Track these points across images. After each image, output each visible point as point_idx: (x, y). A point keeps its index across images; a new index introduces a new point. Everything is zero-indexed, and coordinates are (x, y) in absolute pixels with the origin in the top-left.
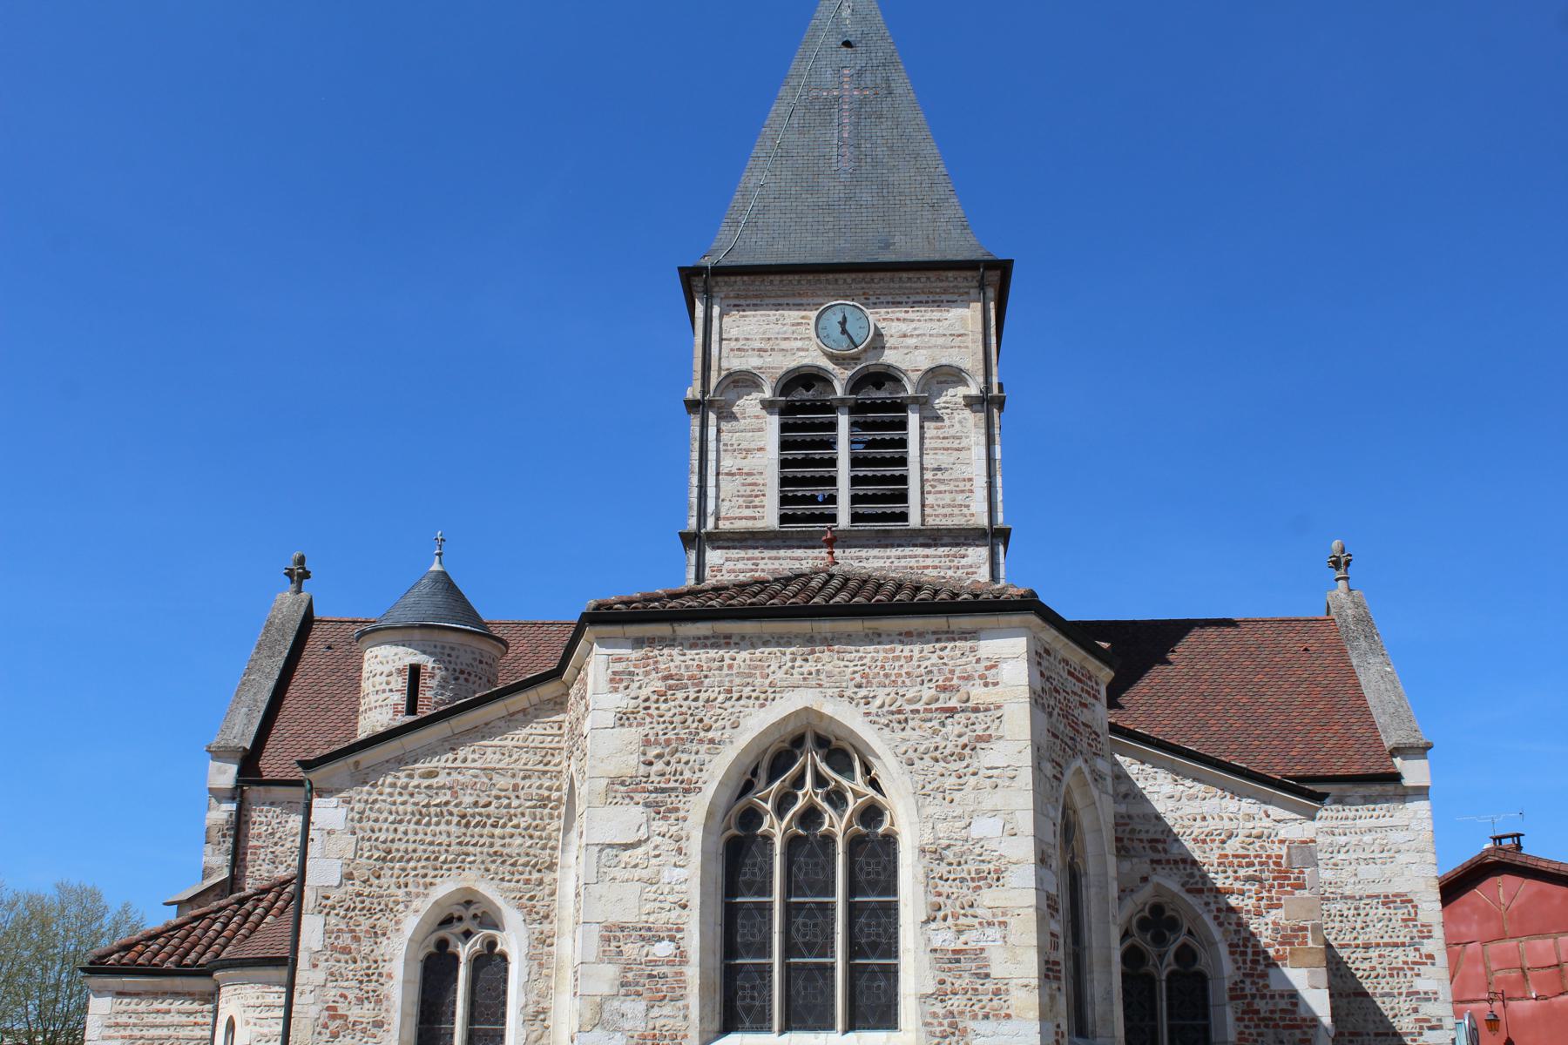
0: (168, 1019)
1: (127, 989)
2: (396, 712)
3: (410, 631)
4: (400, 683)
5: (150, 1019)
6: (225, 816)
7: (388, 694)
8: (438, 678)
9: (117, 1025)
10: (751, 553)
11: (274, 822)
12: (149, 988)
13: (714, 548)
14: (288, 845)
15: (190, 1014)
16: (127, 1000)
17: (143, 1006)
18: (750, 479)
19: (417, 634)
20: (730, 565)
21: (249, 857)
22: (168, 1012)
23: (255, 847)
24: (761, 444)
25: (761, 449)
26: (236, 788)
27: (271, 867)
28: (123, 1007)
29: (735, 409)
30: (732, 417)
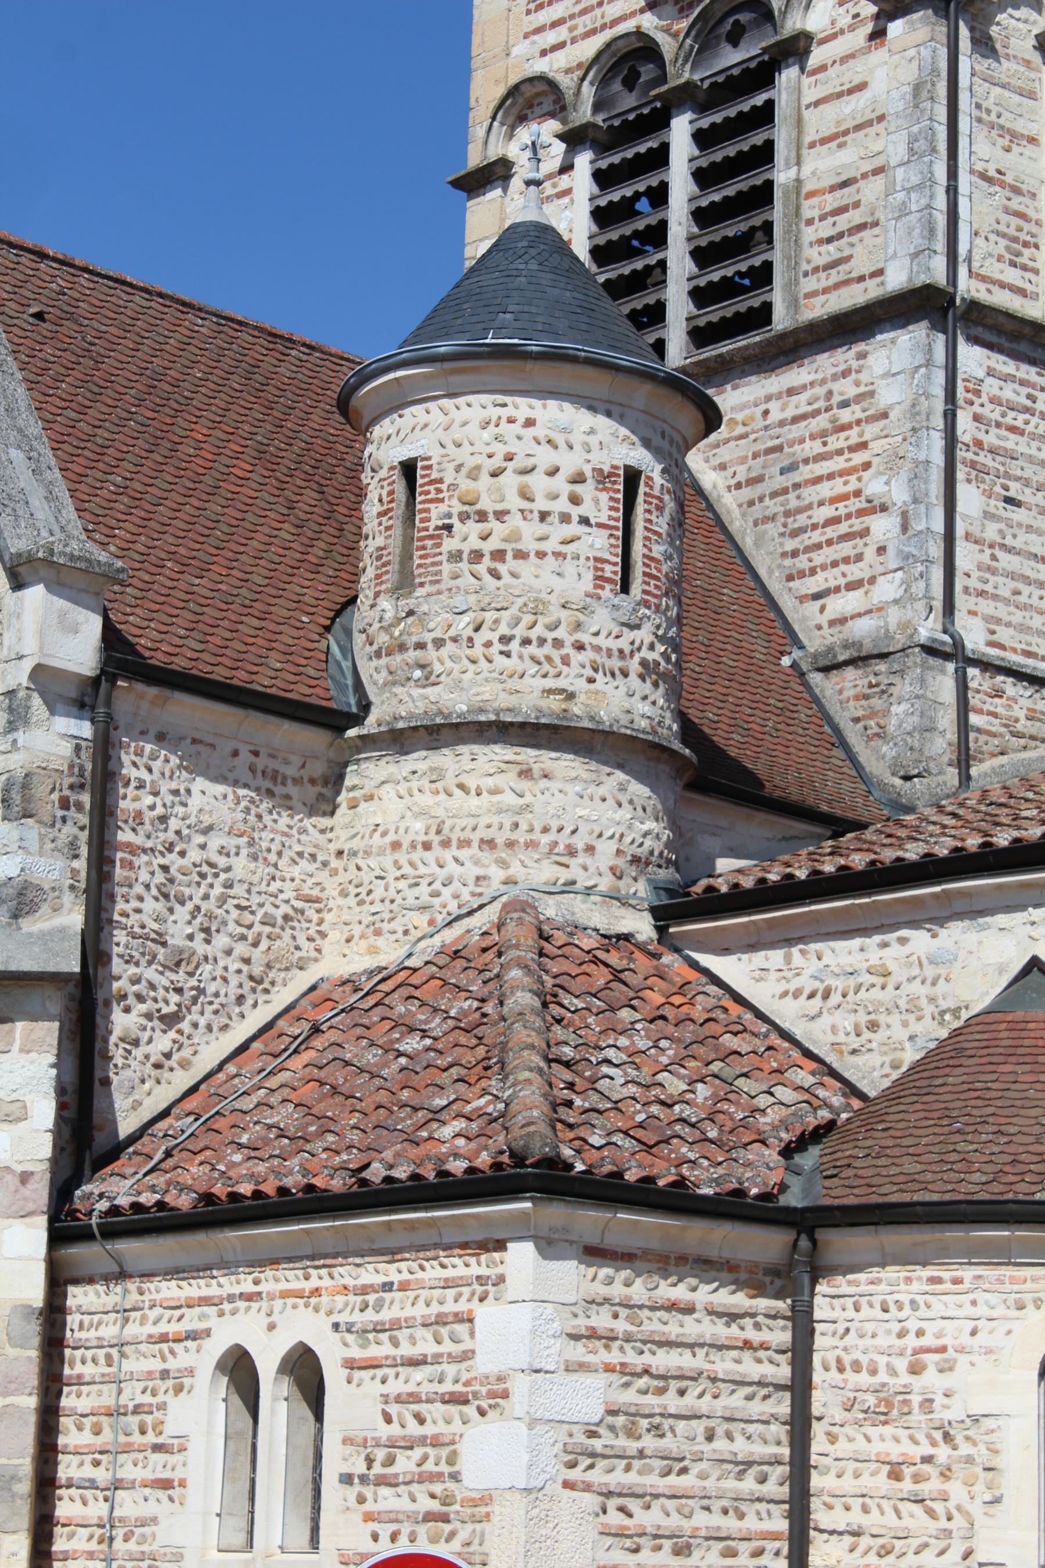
0: (692, 1328)
1: (613, 1240)
2: (600, 579)
3: (634, 382)
4: (601, 505)
5: (653, 1324)
6: (66, 749)
7: (574, 529)
8: (667, 512)
9: (593, 1335)
10: (1027, 372)
11: (165, 787)
12: (654, 1244)
13: (974, 340)
14: (194, 855)
15: (732, 1317)
16: (605, 1272)
17: (639, 1290)
18: (1015, 204)
19: (642, 393)
20: (991, 386)
21: (119, 873)
22: (689, 1310)
23: (134, 850)
24: (1032, 129)
25: (1032, 140)
26: (96, 682)
27: (160, 906)
28: (600, 1290)
29: (994, 31)
30: (984, 45)
